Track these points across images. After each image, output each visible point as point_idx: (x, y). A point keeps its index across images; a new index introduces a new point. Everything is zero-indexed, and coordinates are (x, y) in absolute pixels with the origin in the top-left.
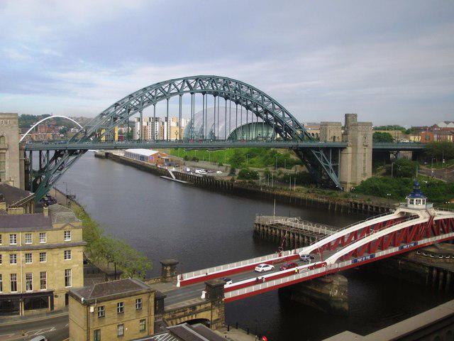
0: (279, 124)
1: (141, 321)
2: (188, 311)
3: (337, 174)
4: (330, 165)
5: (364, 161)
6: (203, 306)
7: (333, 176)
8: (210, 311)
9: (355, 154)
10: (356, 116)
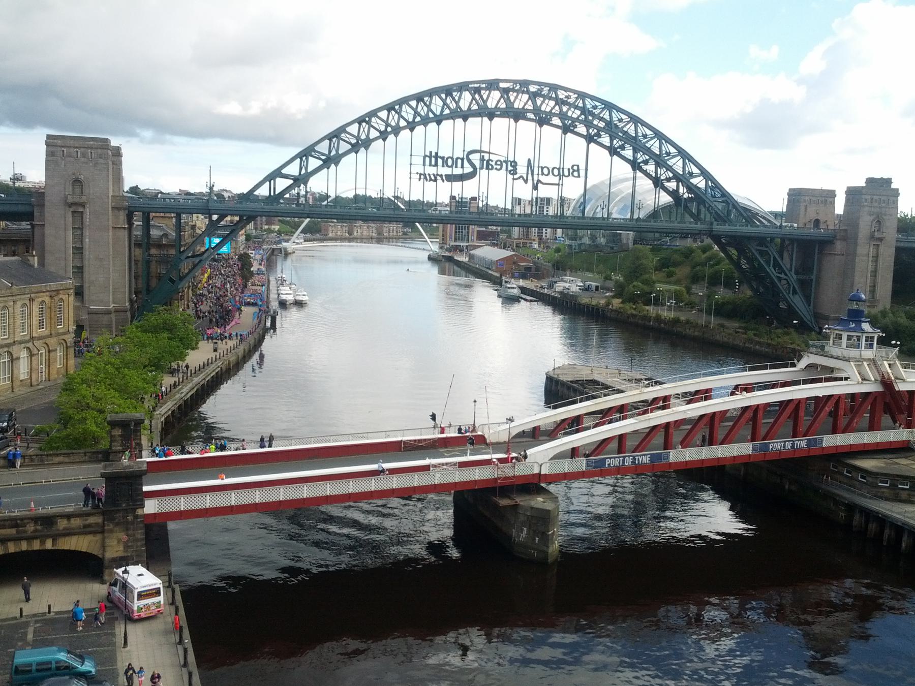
0: (682, 190)
2: (31, 528)
3: (807, 298)
4: (793, 277)
5: (875, 273)
6: (76, 522)
7: (798, 302)
8: (99, 537)
9: (851, 256)
10: (888, 181)
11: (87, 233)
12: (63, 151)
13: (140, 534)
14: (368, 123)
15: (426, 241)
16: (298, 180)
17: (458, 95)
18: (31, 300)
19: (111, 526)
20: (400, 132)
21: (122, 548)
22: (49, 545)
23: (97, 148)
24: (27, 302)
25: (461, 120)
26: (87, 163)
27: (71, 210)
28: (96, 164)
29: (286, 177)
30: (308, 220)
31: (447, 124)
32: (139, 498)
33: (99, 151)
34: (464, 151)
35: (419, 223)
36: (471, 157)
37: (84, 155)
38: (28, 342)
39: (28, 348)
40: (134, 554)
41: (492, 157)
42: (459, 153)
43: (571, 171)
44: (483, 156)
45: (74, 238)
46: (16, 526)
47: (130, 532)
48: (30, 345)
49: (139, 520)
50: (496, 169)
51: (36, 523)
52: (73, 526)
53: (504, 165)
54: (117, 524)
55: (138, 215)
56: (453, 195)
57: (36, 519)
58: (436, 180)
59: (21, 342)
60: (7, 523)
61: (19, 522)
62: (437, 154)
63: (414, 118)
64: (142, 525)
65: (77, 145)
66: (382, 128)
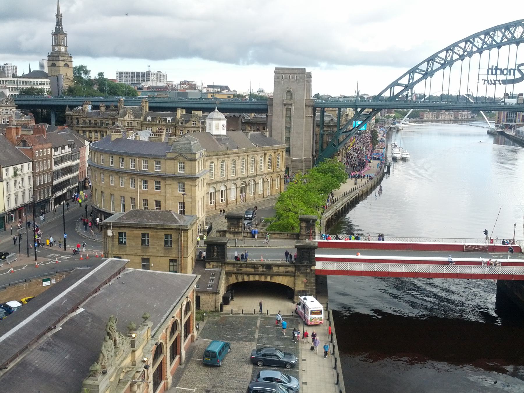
1: (171, 261)
2: (261, 269)
6: (282, 269)
8: (292, 278)
11: (292, 119)
12: (283, 76)
13: (313, 280)
14: (452, 50)
15: (487, 122)
16: (407, 87)
17: (514, 29)
18: (265, 154)
19: (299, 274)
20: (472, 55)
21: (303, 286)
22: (269, 279)
23: (299, 74)
24: (263, 155)
25: (515, 45)
26: (294, 82)
27: (286, 107)
28: (298, 82)
29: (400, 85)
30: (412, 110)
31: (505, 48)
32: (313, 261)
33: (300, 75)
34: (516, 64)
35: (482, 110)
36: (520, 68)
37: (292, 78)
38: (262, 175)
39: (263, 178)
40: (309, 290)
42: (512, 66)
45: (286, 122)
46: (254, 267)
47: (308, 278)
48: (264, 177)
49: (313, 272)
51: (263, 267)
52: (280, 271)
54: (302, 273)
55: (318, 110)
56: (506, 92)
57: (263, 265)
58: (495, 84)
59: (259, 175)
60: (250, 266)
61: (255, 265)
62: (497, 67)
63: (483, 45)
64: (314, 275)
65: (289, 73)
66: (461, 53)
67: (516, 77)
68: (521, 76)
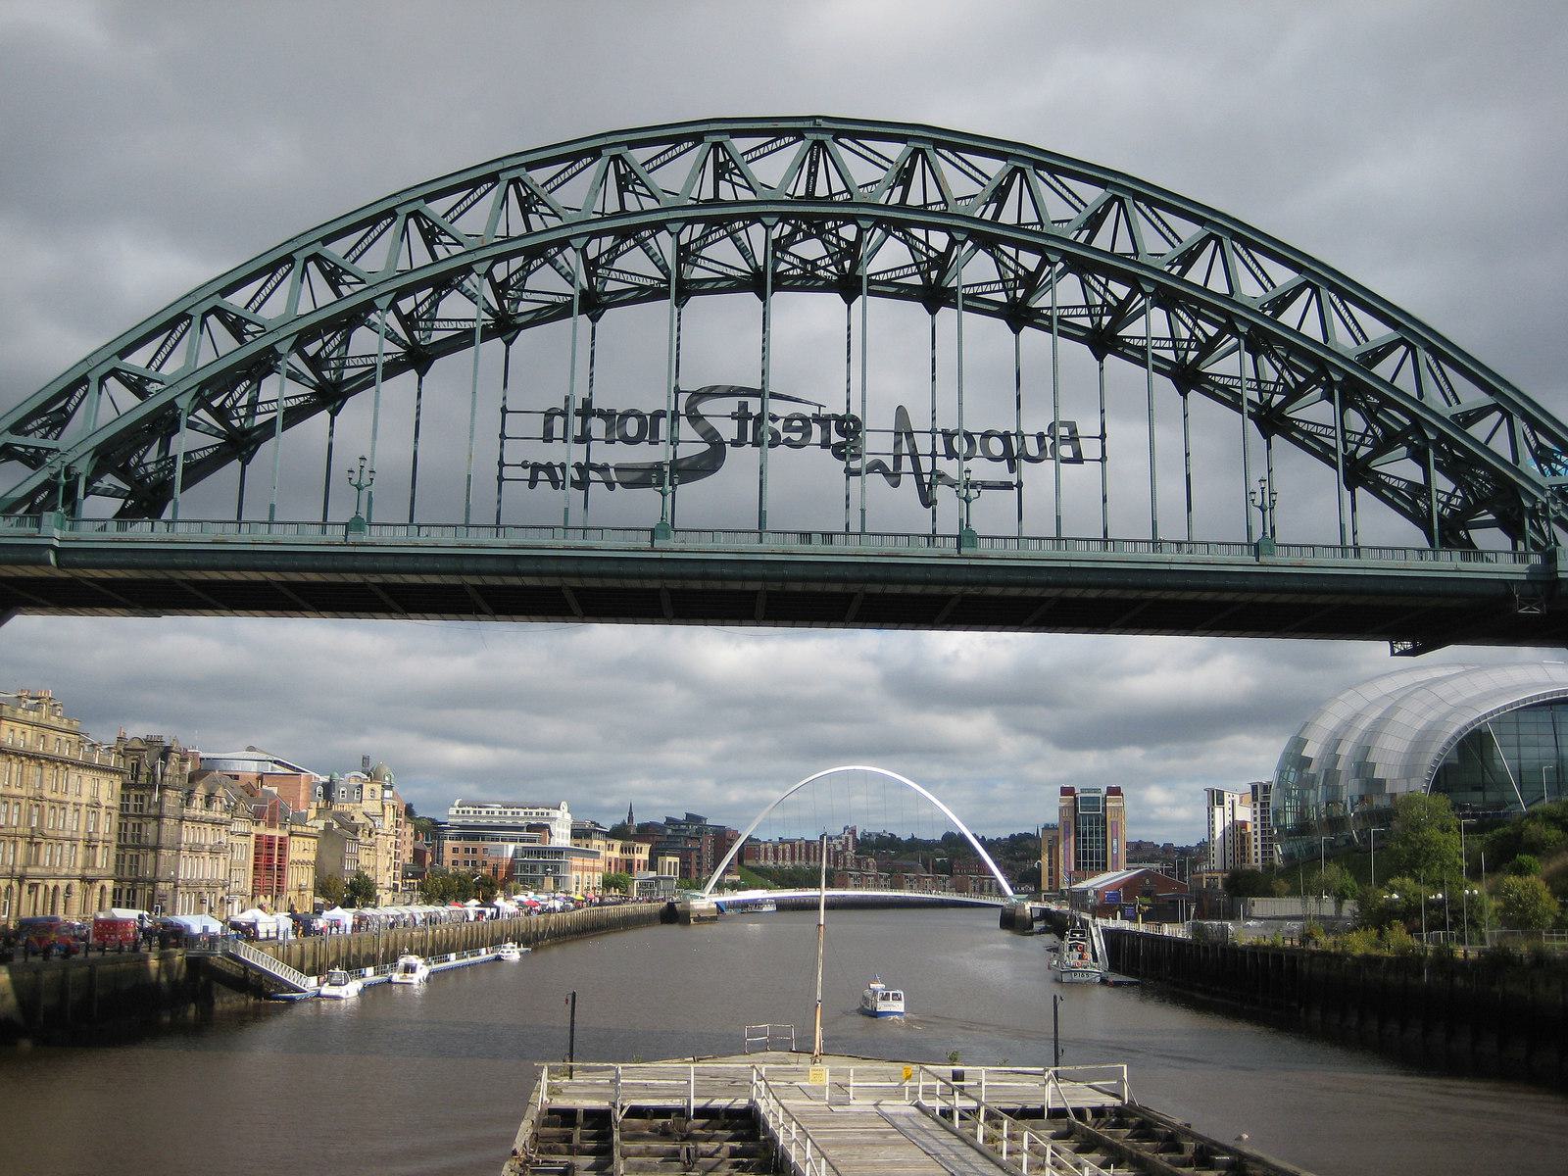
34: (677, 391)
36: (703, 408)
41: (777, 407)
43: (1048, 441)
44: (744, 406)
50: (789, 443)
53: (816, 428)
58: (583, 484)
62: (587, 403)
67: (685, 451)
68: (707, 447)
